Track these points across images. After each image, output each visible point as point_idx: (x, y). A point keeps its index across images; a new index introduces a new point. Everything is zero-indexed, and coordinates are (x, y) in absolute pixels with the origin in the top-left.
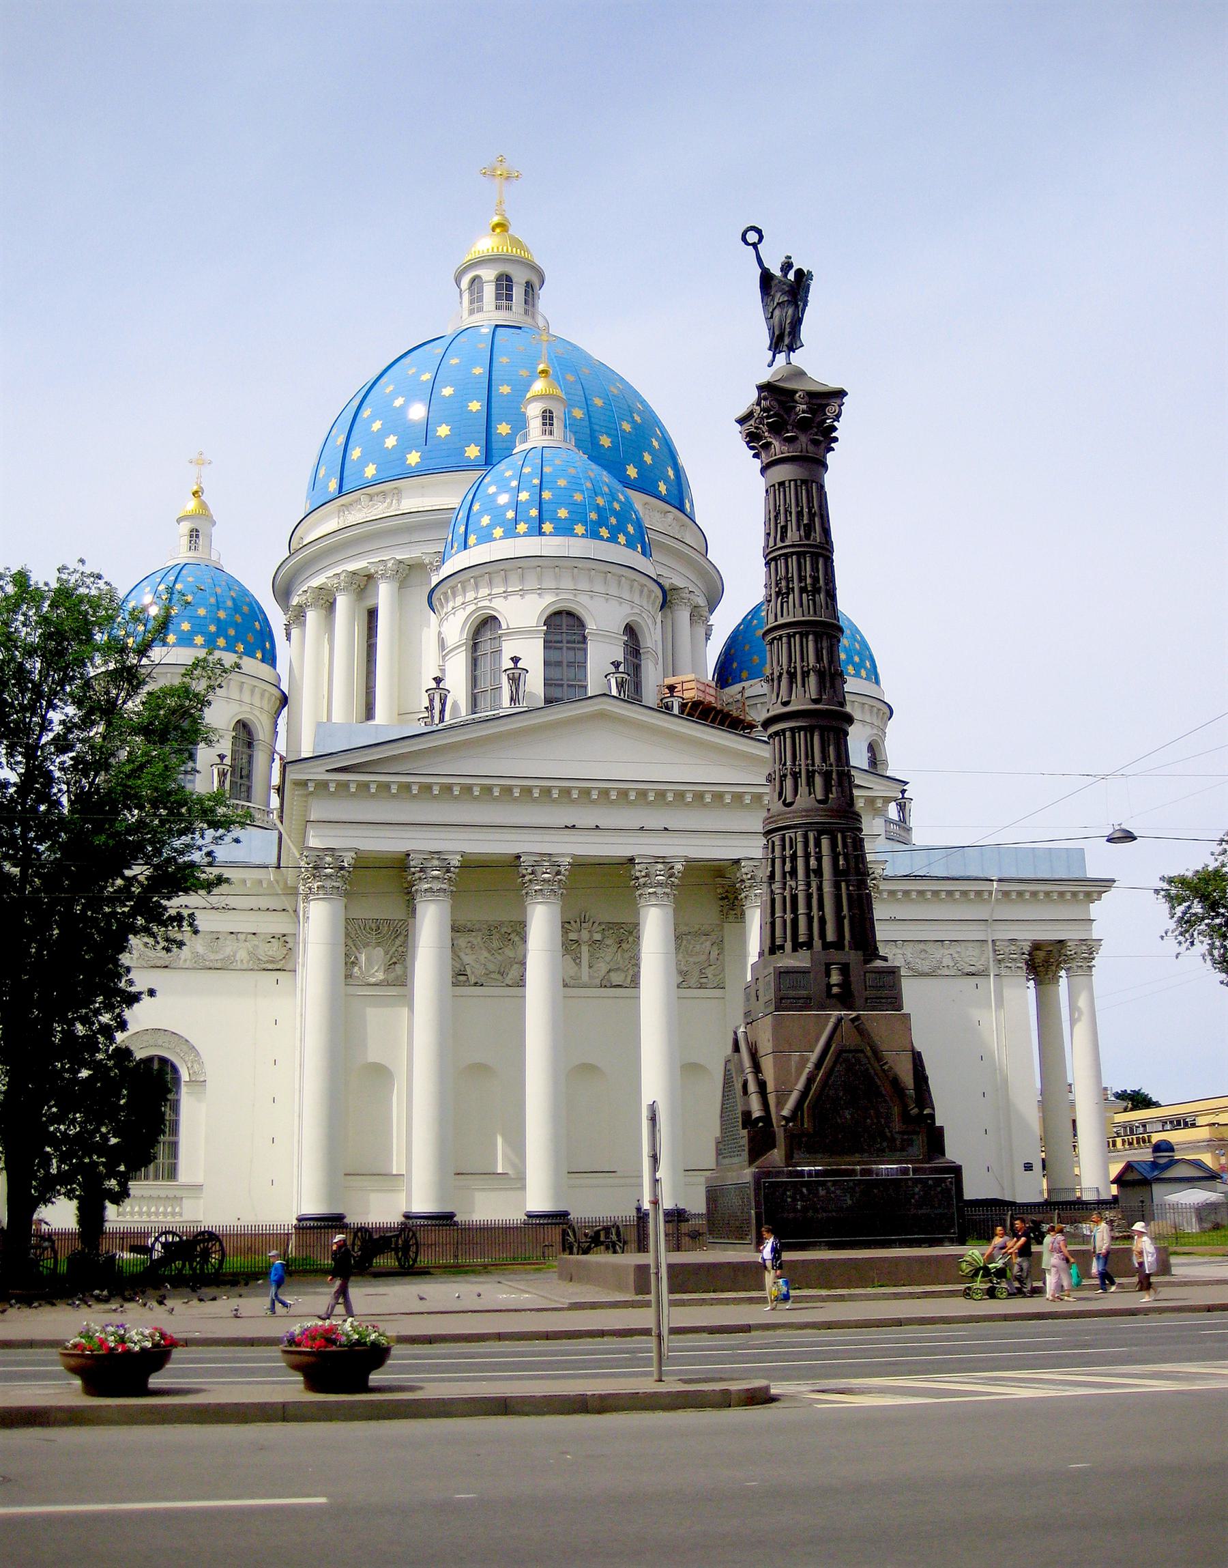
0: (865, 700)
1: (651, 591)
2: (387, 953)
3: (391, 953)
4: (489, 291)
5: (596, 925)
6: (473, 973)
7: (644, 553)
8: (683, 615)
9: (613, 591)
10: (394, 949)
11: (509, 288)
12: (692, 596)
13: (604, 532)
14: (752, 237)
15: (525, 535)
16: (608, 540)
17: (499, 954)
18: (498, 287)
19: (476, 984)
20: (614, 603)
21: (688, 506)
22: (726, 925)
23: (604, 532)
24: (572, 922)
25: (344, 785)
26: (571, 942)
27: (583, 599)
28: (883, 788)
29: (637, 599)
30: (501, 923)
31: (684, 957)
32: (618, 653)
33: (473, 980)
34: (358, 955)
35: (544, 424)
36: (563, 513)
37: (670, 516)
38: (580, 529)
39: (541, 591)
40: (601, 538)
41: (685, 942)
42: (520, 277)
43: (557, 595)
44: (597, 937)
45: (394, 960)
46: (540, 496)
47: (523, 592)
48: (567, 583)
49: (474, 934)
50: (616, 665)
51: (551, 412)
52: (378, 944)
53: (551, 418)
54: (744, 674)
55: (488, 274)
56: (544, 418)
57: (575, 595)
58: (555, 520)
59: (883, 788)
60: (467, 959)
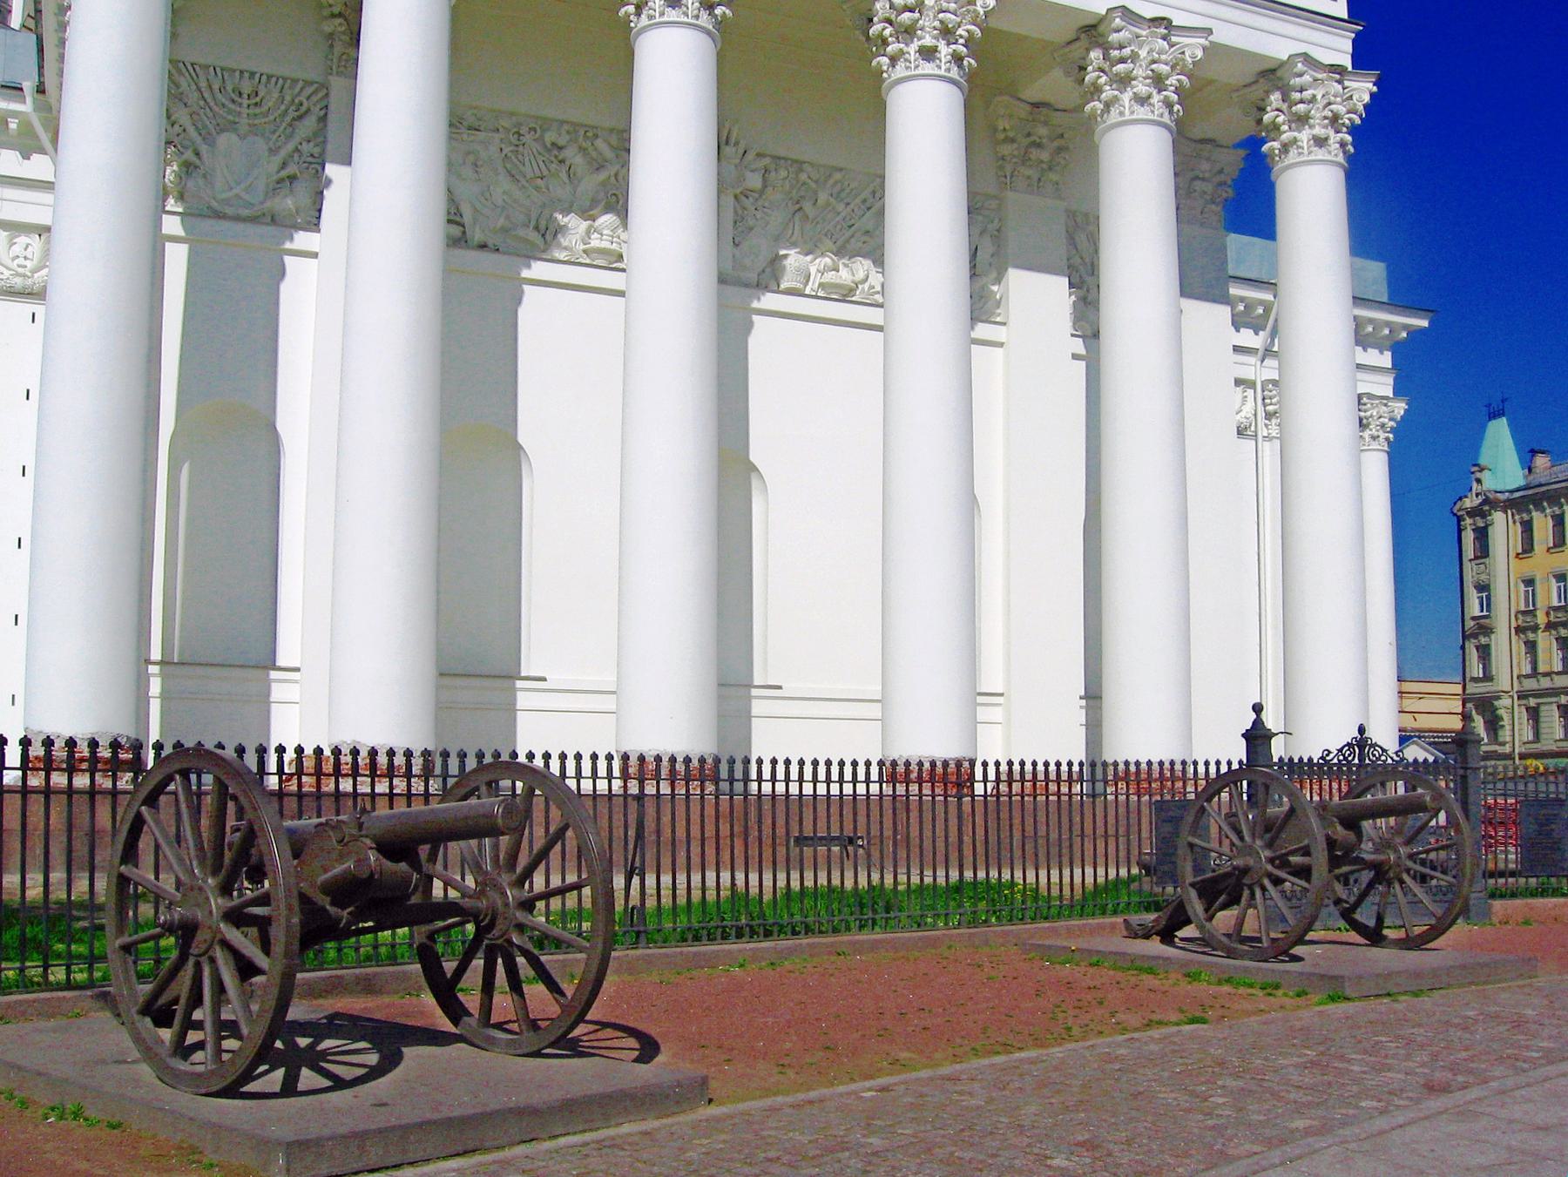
2: (273, 151)
3: (283, 153)
5: (750, 156)
6: (475, 221)
10: (290, 146)
17: (537, 189)
19: (483, 246)
22: (1010, 195)
30: (546, 124)
33: (477, 236)
34: (204, 149)
44: (754, 181)
45: (292, 169)
49: (481, 136)
52: (254, 130)
60: (466, 191)
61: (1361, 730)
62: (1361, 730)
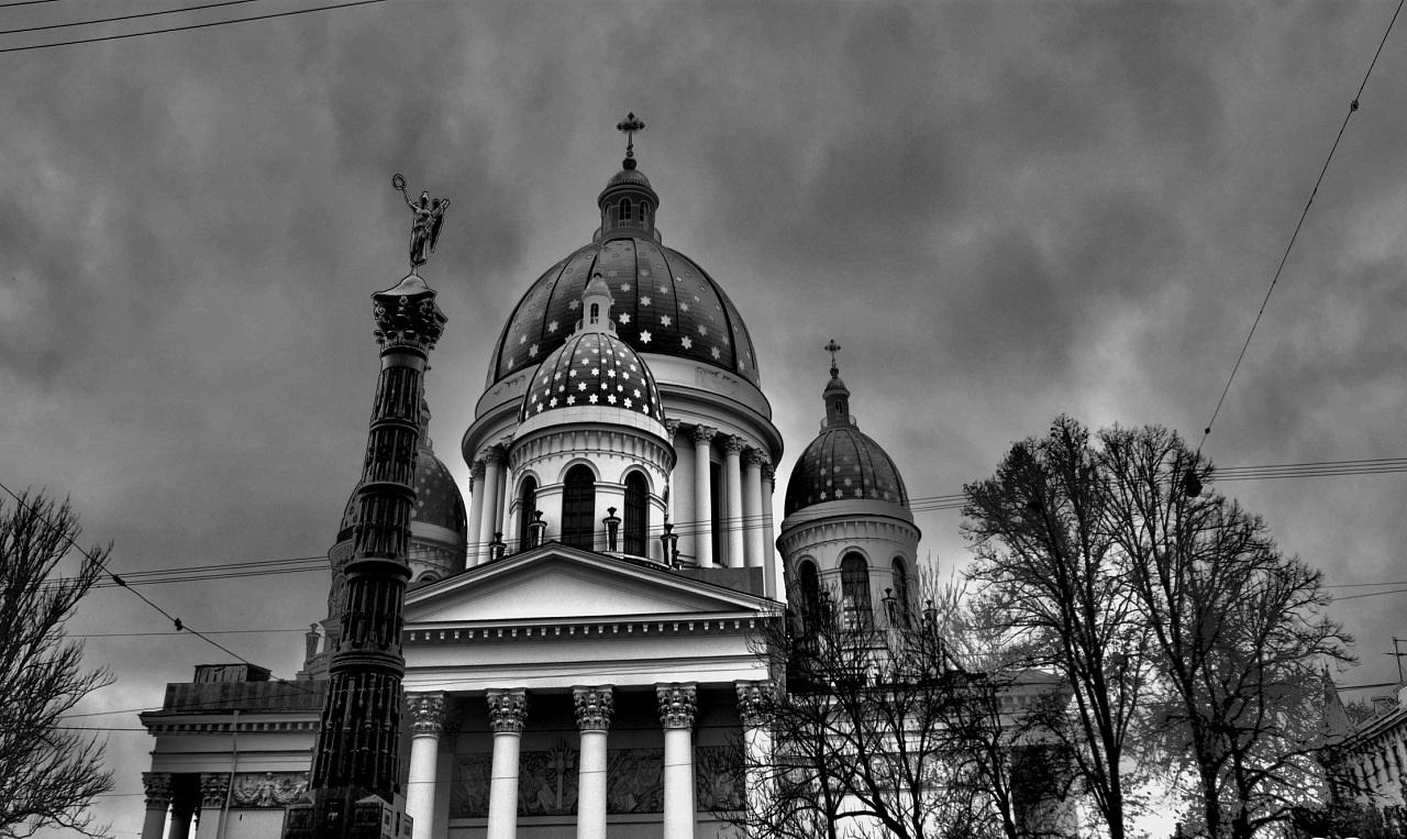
0: (893, 521)
1: (659, 448)
8: (735, 461)
12: (739, 442)
13: (612, 399)
14: (399, 183)
16: (615, 405)
20: (617, 459)
23: (612, 399)
27: (592, 457)
29: (639, 454)
32: (618, 501)
35: (592, 315)
38: (594, 398)
43: (573, 455)
46: (568, 373)
48: (580, 446)
50: (612, 510)
53: (597, 310)
54: (797, 505)
57: (586, 454)
58: (577, 393)
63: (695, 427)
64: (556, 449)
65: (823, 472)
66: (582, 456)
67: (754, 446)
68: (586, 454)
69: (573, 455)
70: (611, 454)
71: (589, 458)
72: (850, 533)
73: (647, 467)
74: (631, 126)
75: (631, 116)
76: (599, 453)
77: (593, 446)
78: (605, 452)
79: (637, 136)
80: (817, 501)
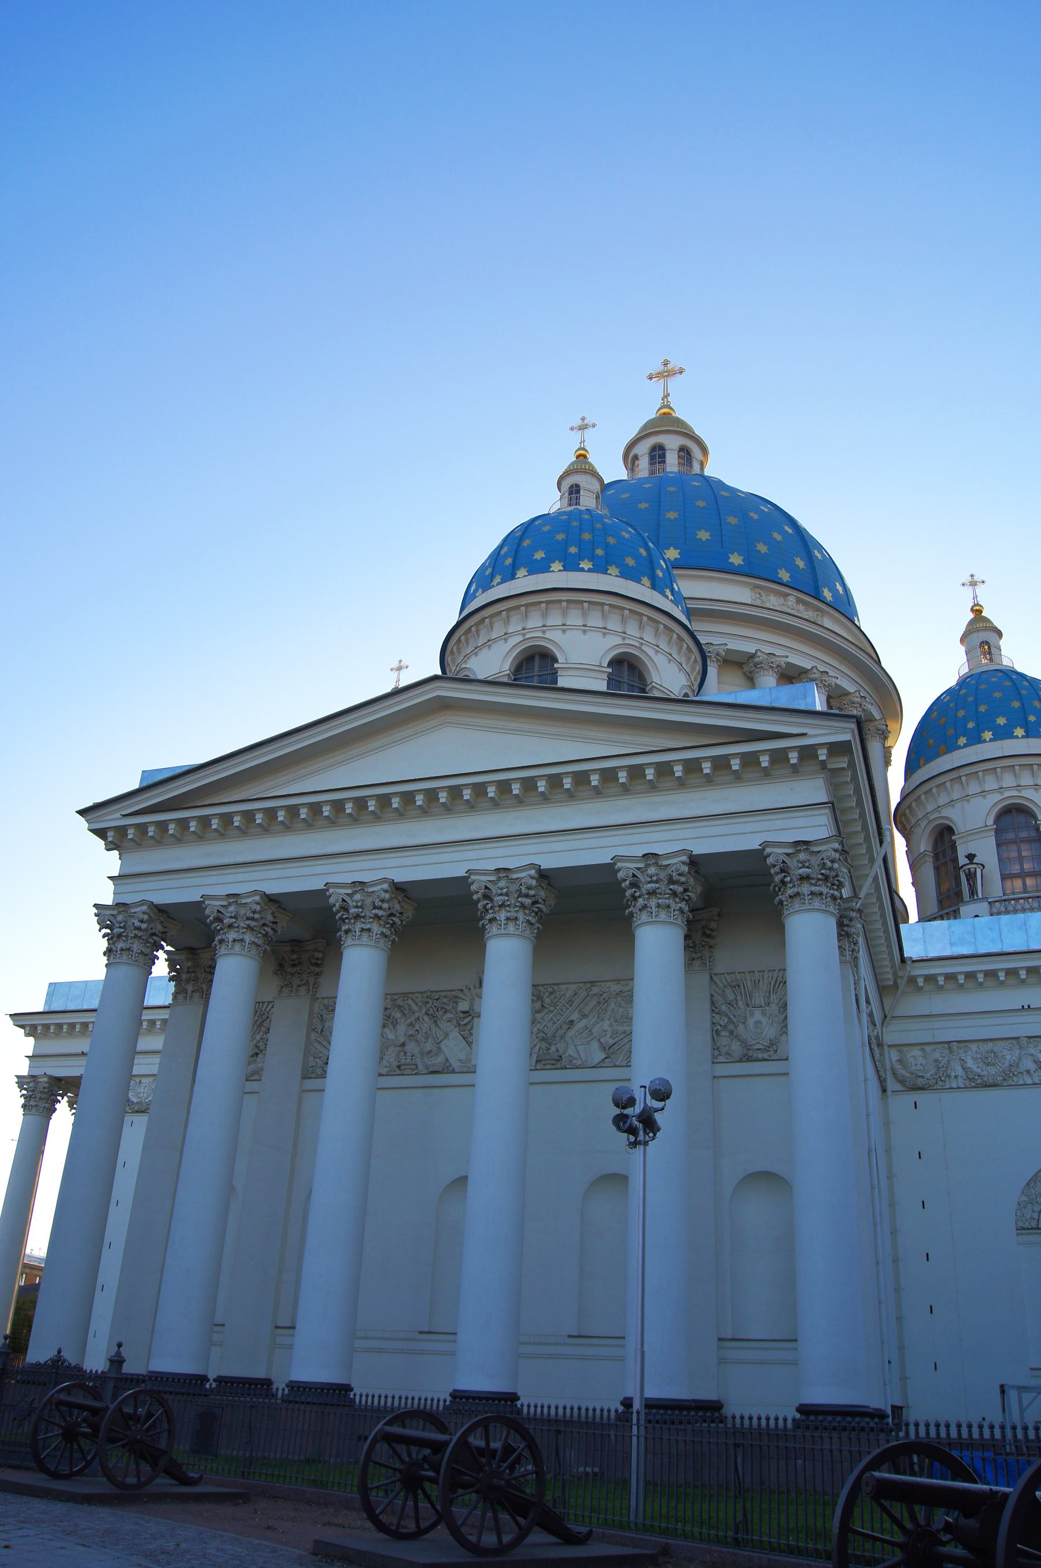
4: (644, 463)
7: (654, 587)
9: (595, 620)
11: (663, 456)
15: (498, 584)
16: (590, 570)
18: (652, 458)
21: (827, 594)
24: (466, 991)
25: (142, 828)
26: (462, 1015)
28: (822, 732)
31: (611, 1025)
36: (539, 555)
37: (791, 601)
39: (506, 637)
40: (582, 570)
41: (613, 1005)
42: (672, 443)
43: (524, 635)
47: (489, 643)
48: (534, 621)
51: (577, 486)
53: (578, 492)
54: (922, 762)
55: (643, 449)
56: (570, 493)
57: (544, 632)
59: (822, 732)
61: (59, 1352)
62: (59, 1352)
63: (752, 656)
64: (497, 631)
65: (961, 713)
66: (540, 634)
67: (850, 688)
68: (544, 632)
69: (524, 635)
70: (585, 629)
71: (549, 635)
72: (1008, 780)
73: (650, 651)
74: (667, 373)
75: (666, 363)
76: (564, 628)
77: (555, 619)
78: (574, 627)
79: (673, 383)
80: (952, 747)
